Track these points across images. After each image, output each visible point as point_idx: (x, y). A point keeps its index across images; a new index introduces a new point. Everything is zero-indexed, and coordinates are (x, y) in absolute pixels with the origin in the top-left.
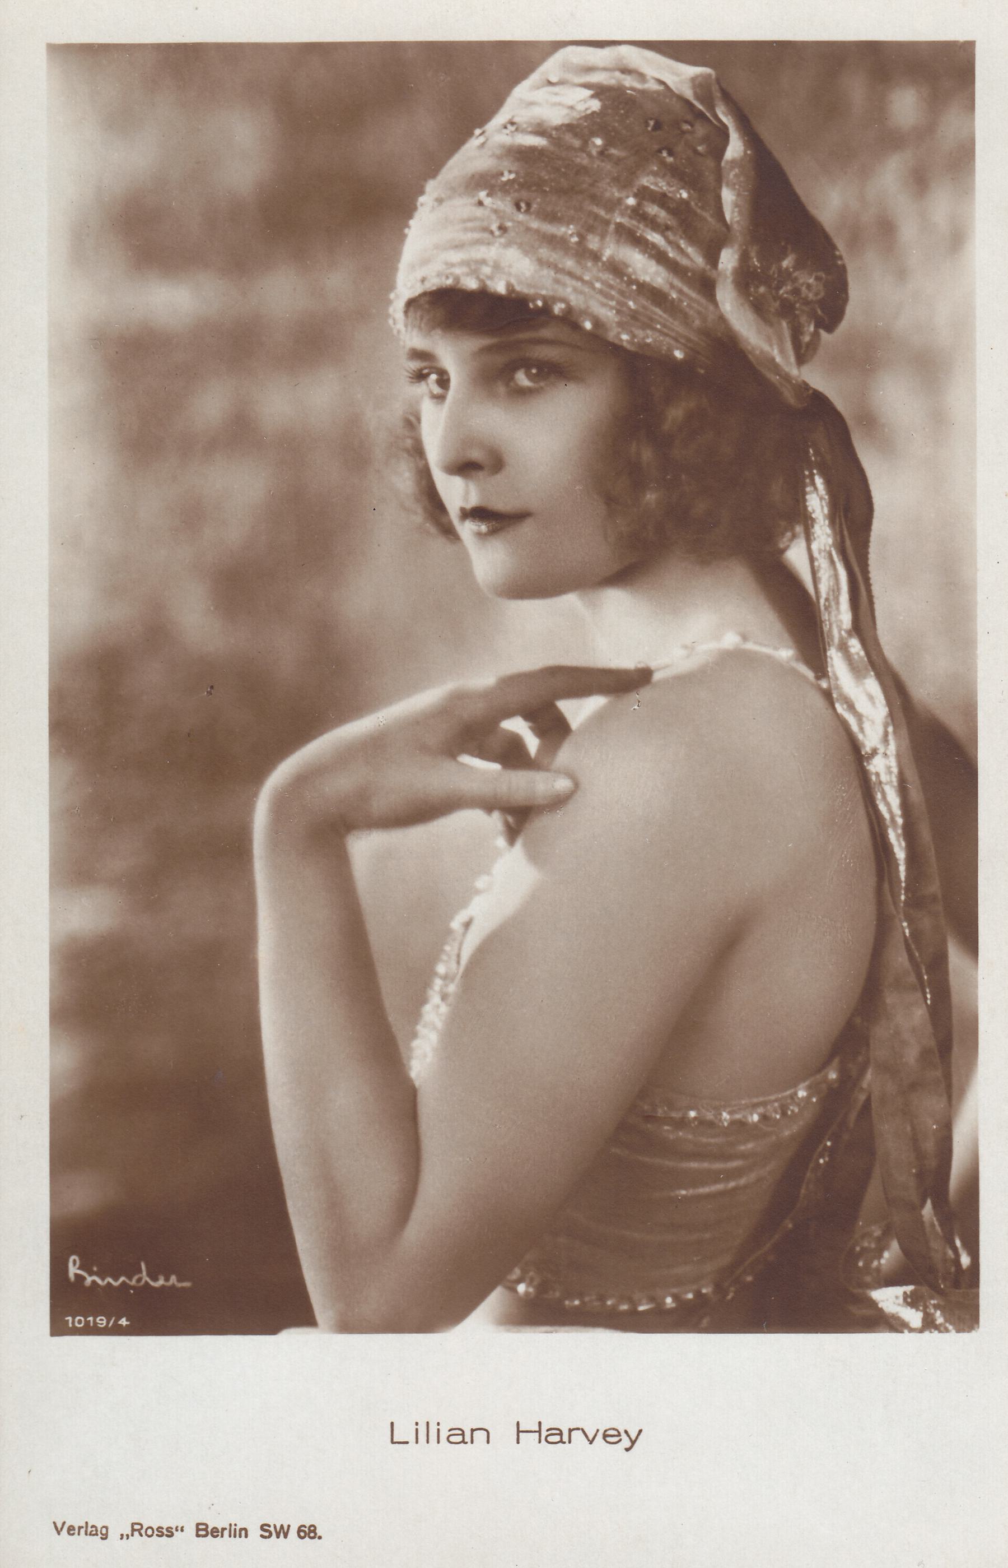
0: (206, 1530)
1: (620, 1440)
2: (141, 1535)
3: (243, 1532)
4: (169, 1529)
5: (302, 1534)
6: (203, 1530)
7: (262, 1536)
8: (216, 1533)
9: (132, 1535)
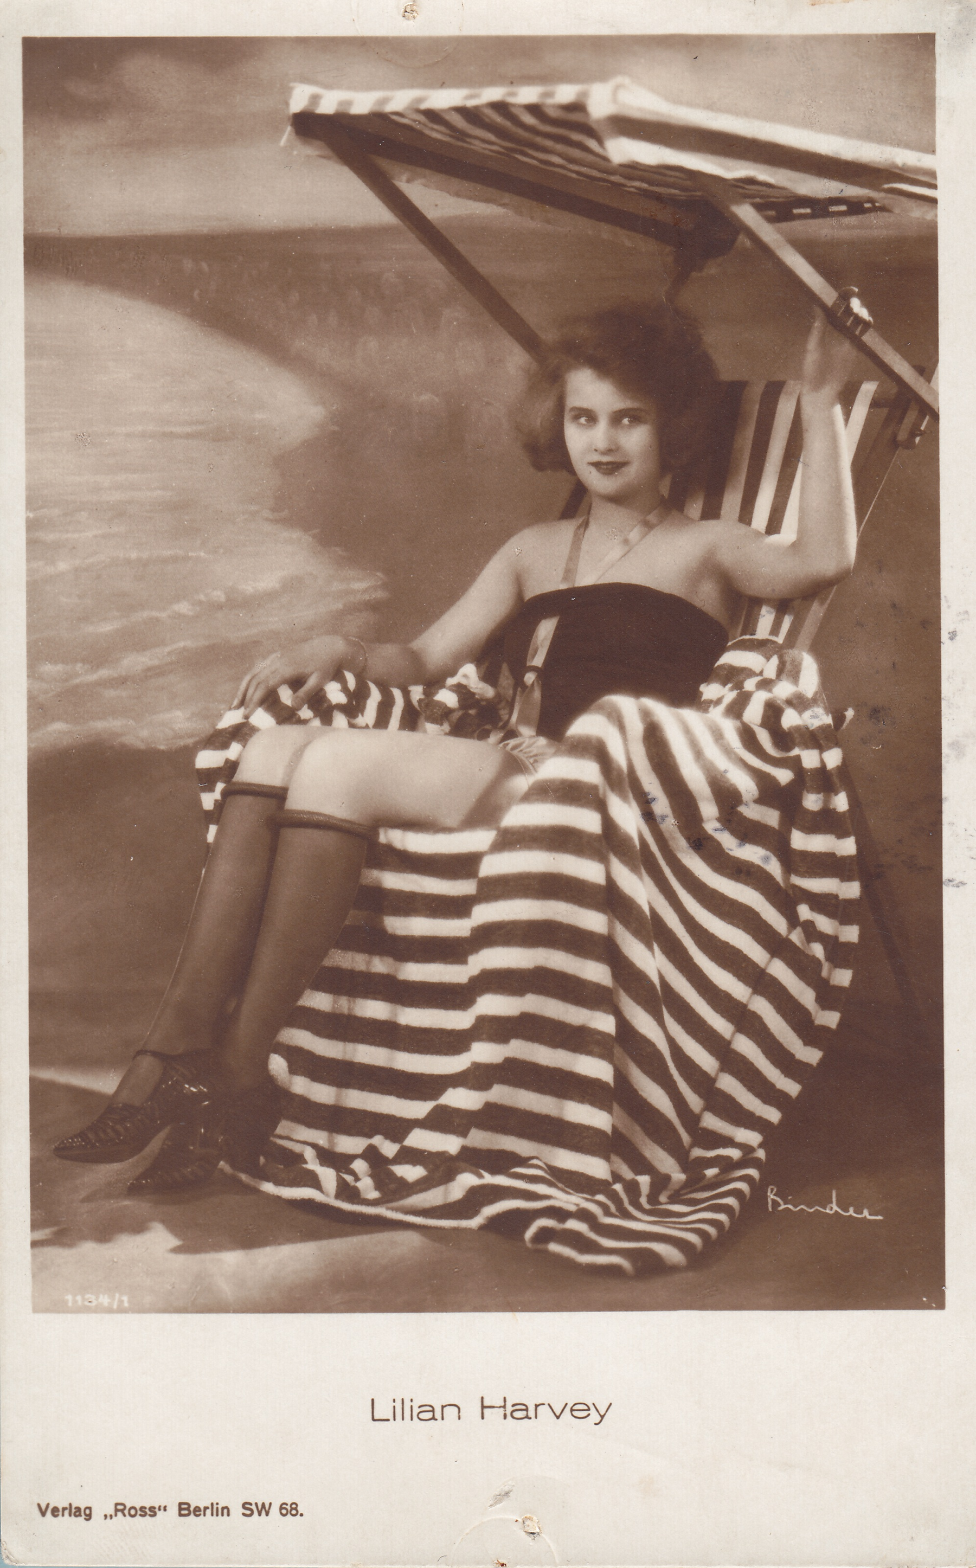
0: (188, 1509)
1: (589, 1415)
2: (125, 1515)
3: (225, 1511)
4: (152, 1509)
5: (284, 1512)
6: (185, 1509)
7: (244, 1515)
8: (197, 1511)
9: (116, 1515)
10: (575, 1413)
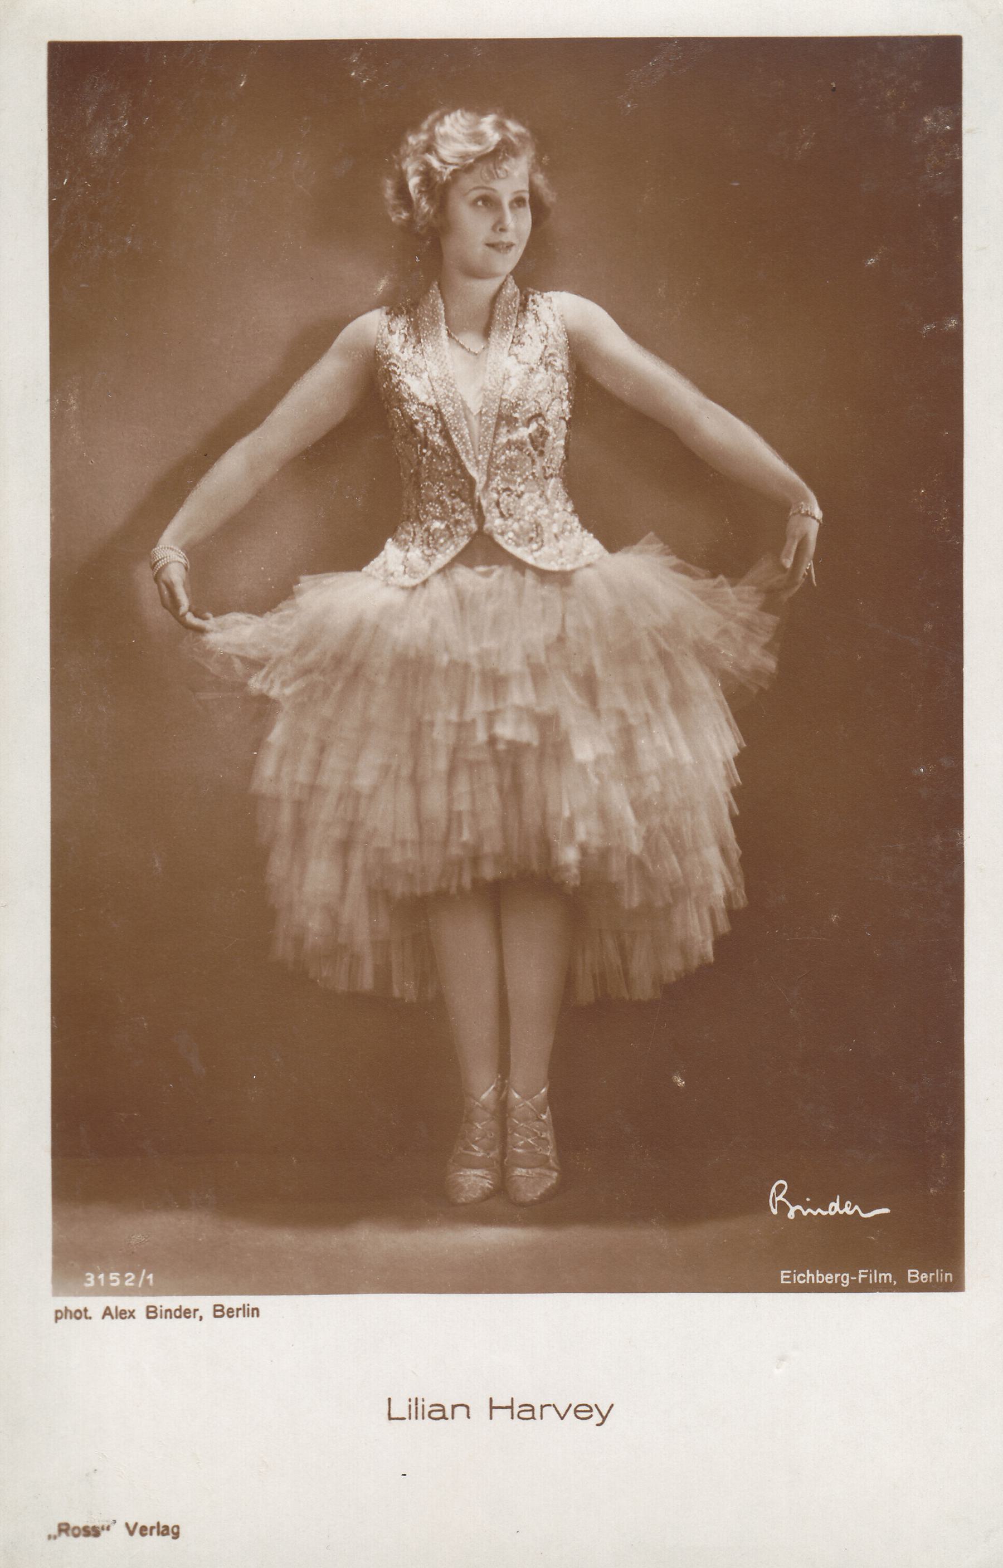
1: (591, 1416)
10: (578, 1414)
